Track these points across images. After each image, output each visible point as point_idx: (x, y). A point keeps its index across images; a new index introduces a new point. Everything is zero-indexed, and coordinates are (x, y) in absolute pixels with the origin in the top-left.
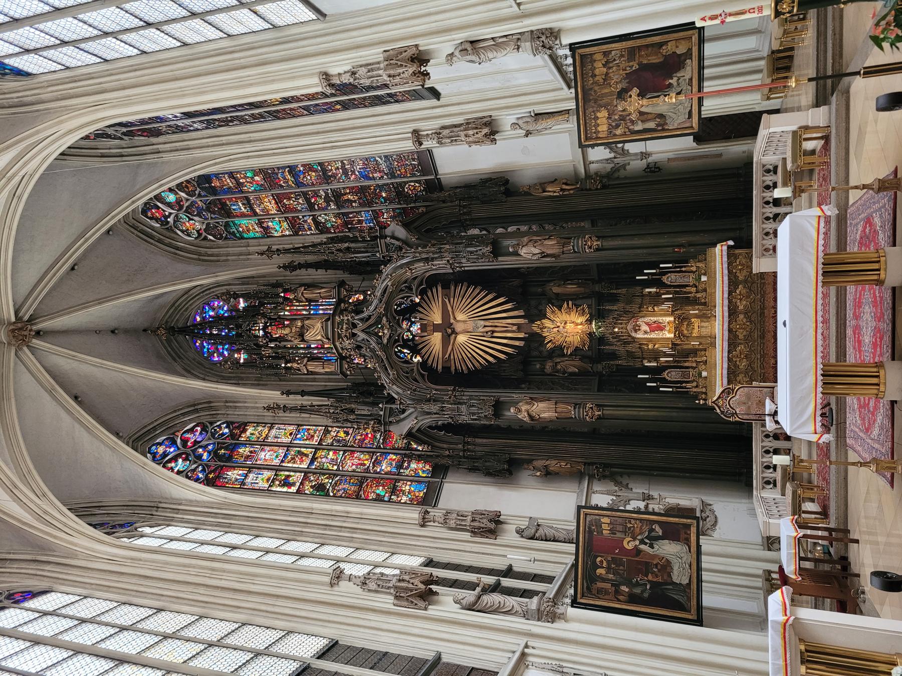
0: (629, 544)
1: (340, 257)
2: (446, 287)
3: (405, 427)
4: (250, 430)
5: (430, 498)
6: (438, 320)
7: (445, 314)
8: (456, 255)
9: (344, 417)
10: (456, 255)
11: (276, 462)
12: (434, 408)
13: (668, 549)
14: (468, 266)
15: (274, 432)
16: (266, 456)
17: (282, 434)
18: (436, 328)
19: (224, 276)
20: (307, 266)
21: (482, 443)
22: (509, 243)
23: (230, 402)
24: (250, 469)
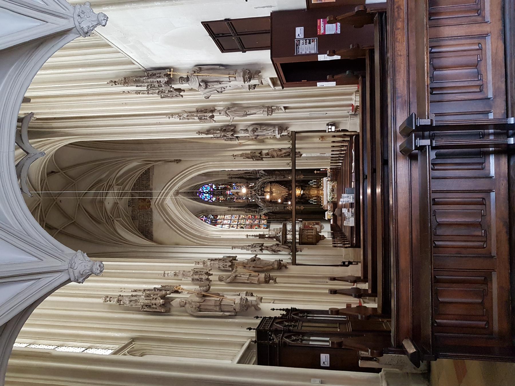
0: (310, 226)
1: (248, 177)
2: (271, 183)
3: (264, 212)
4: (219, 217)
5: (268, 227)
6: (269, 191)
7: (271, 189)
8: (276, 178)
9: (250, 211)
10: (276, 178)
11: (229, 223)
12: (271, 208)
13: (316, 226)
14: (278, 180)
15: (226, 217)
16: (225, 222)
17: (228, 217)
18: (268, 192)
19: (214, 180)
20: (236, 178)
21: (278, 216)
22: (286, 175)
23: (212, 210)
24: (223, 225)
